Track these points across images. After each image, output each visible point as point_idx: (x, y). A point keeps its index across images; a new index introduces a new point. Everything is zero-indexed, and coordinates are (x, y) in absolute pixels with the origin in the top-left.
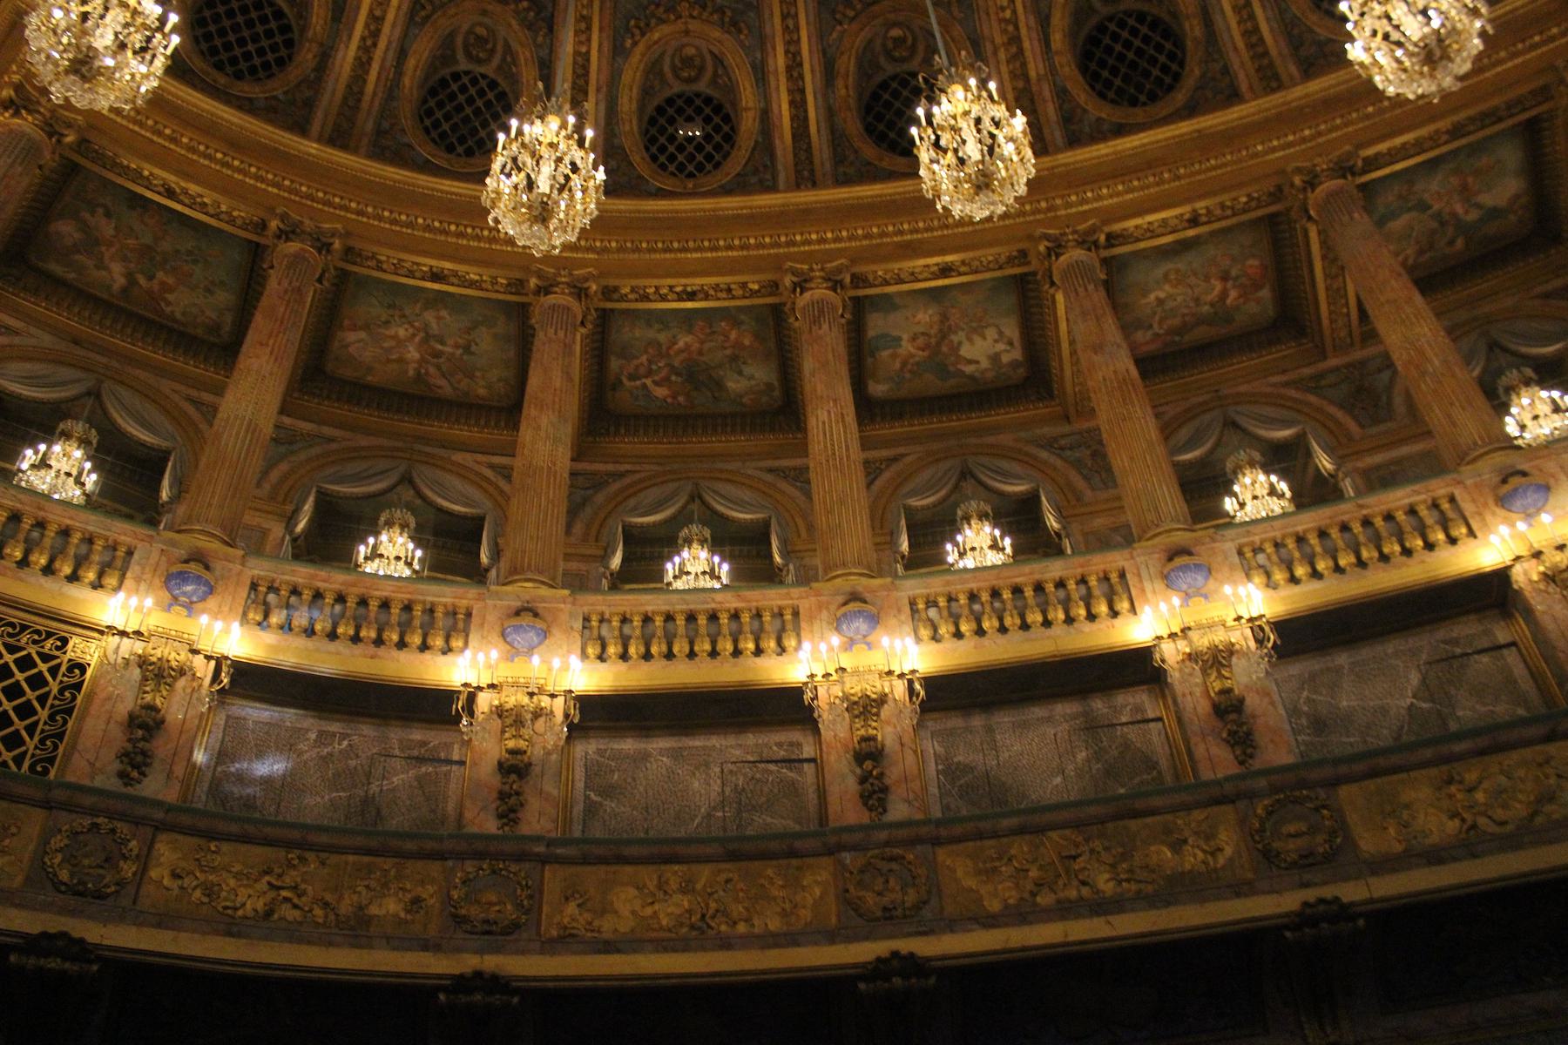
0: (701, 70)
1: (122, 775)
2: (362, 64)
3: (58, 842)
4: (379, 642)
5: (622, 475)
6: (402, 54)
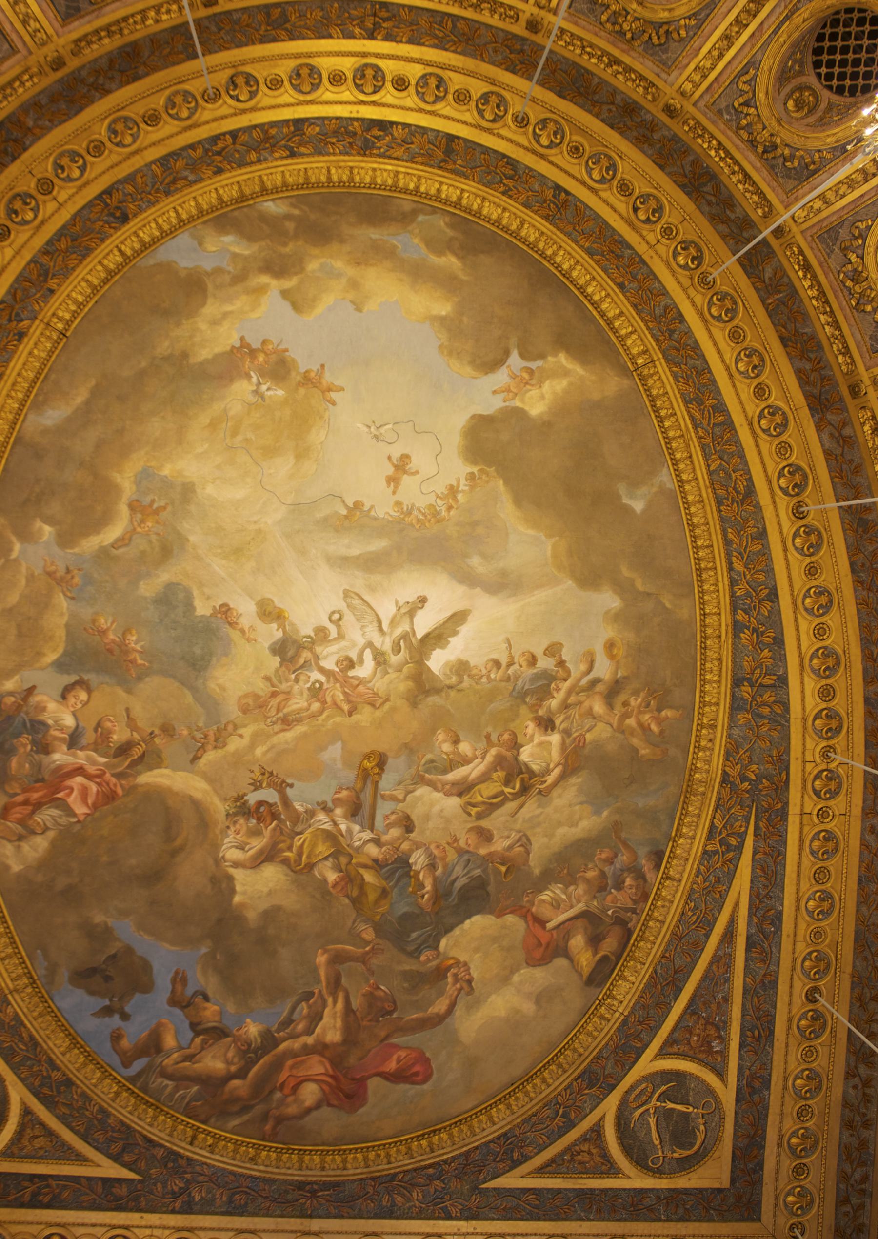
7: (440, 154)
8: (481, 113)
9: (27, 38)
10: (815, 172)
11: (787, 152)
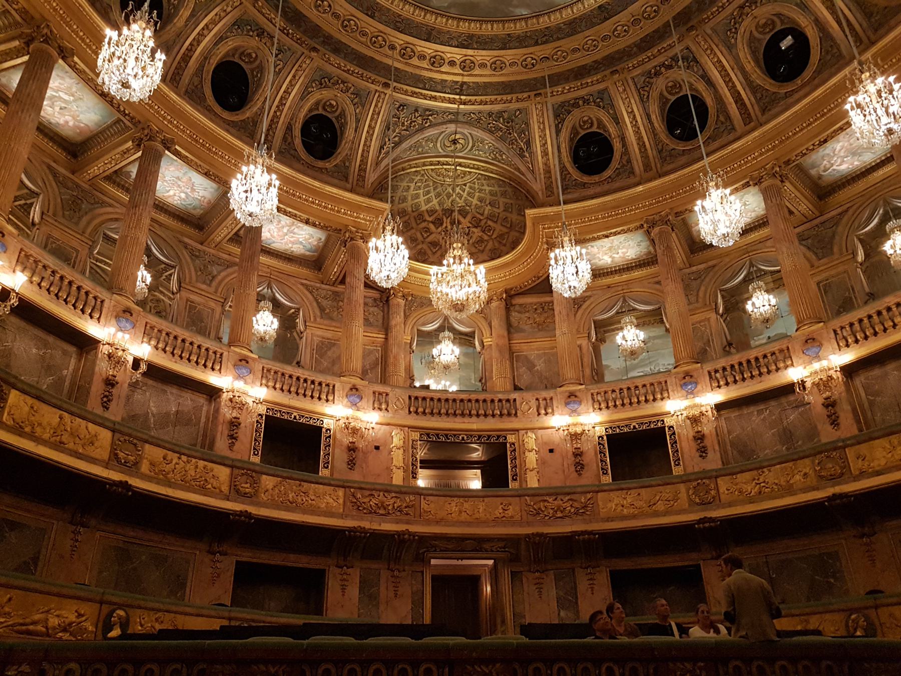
0: (773, 22)
1: (701, 456)
2: (637, 132)
3: (691, 492)
4: (760, 374)
5: (847, 211)
6: (648, 116)
7: (434, 33)
8: (413, 51)
9: (626, 84)
10: (234, 24)
11: (251, 33)
